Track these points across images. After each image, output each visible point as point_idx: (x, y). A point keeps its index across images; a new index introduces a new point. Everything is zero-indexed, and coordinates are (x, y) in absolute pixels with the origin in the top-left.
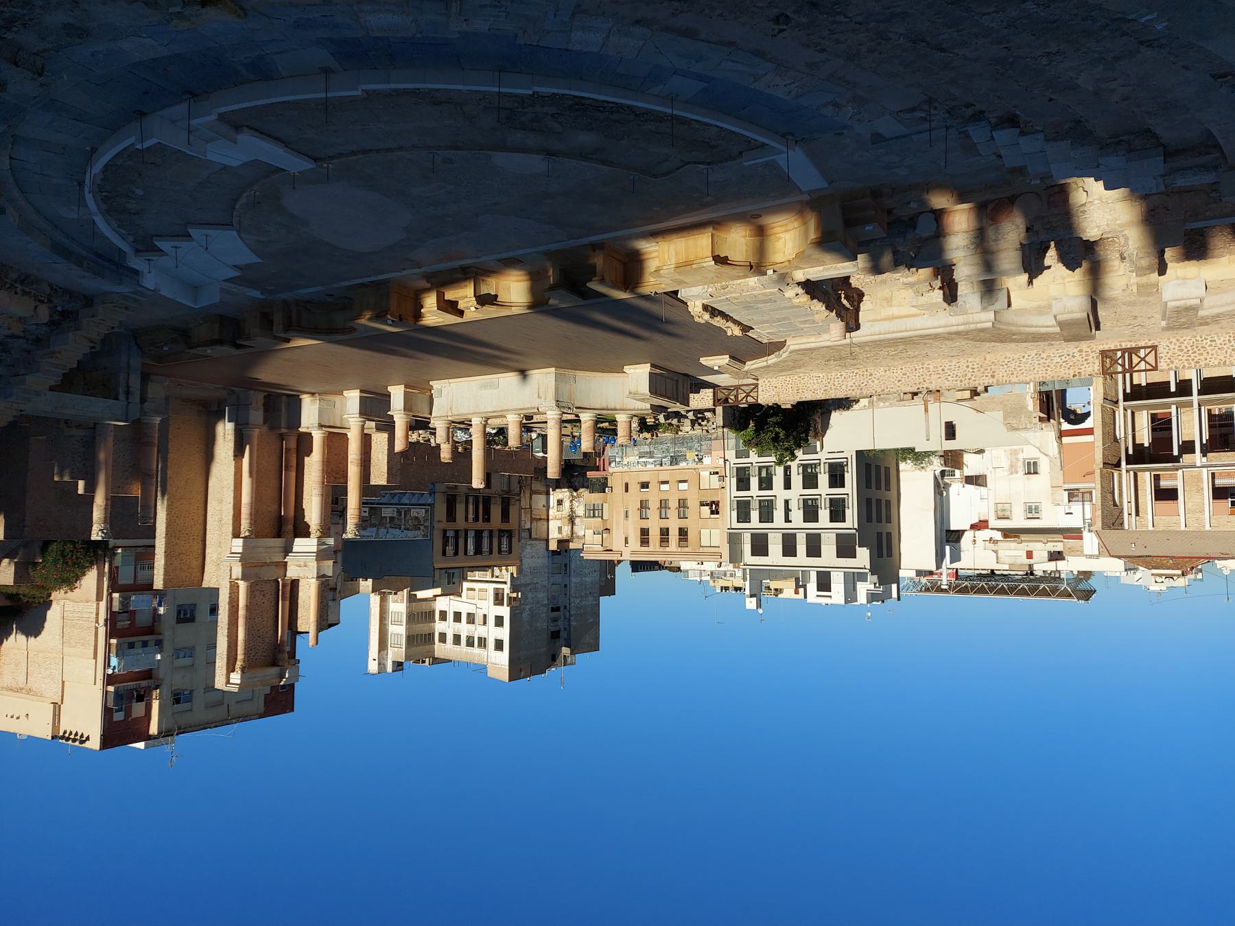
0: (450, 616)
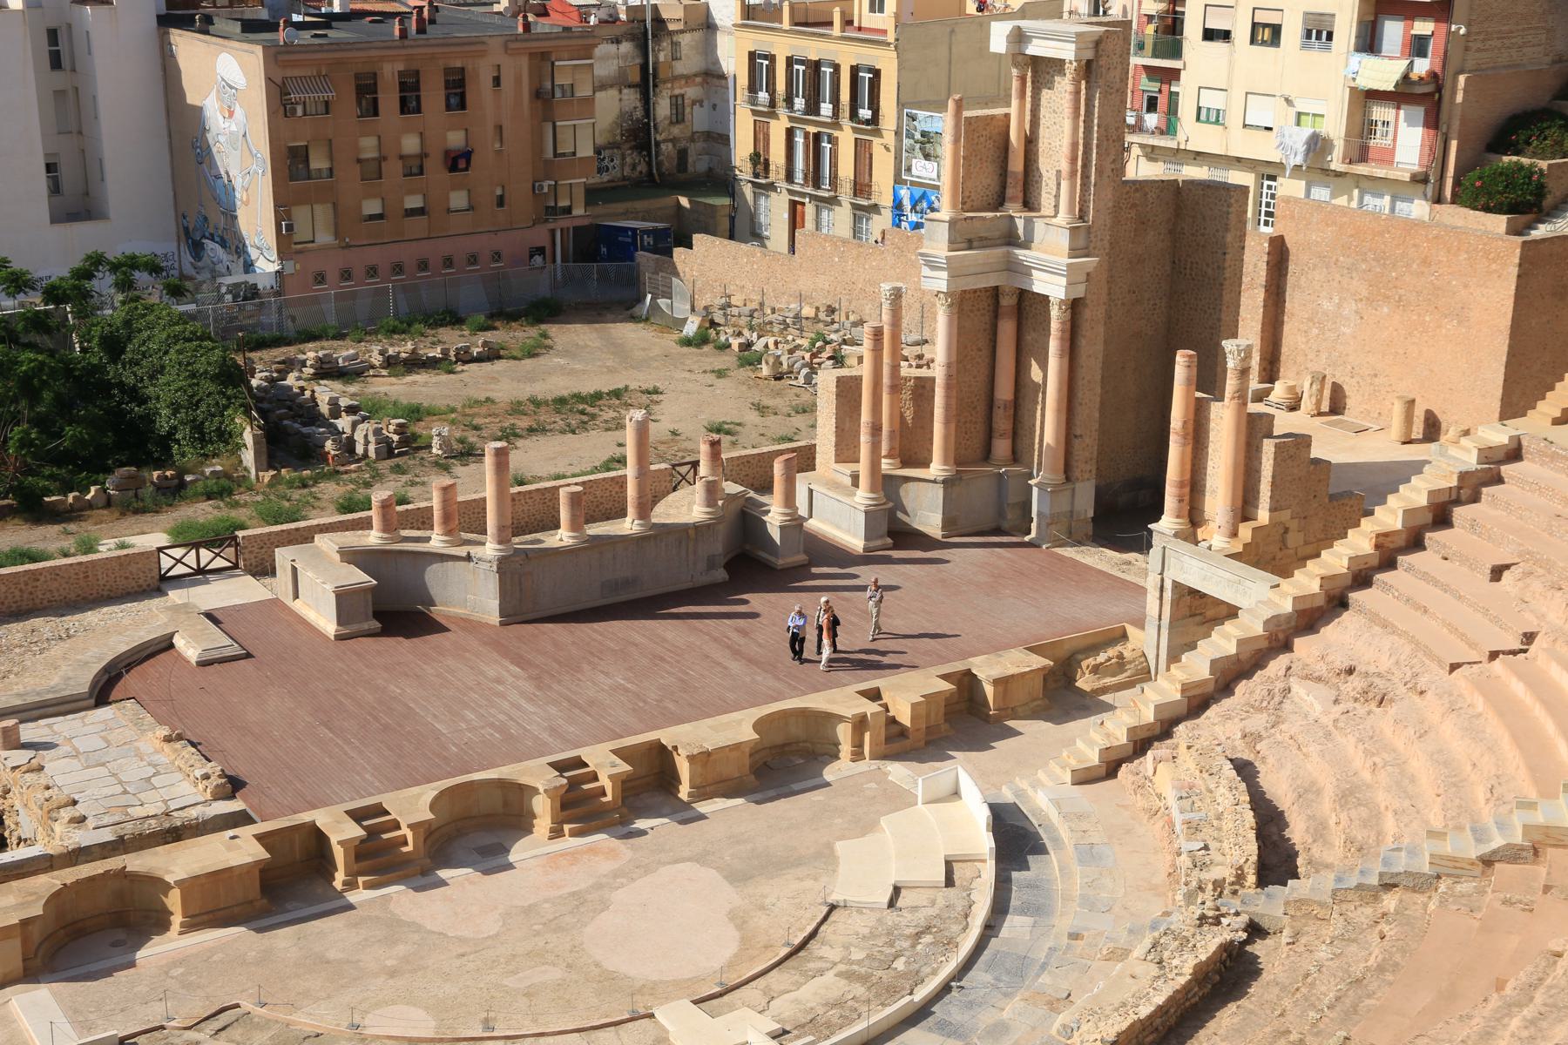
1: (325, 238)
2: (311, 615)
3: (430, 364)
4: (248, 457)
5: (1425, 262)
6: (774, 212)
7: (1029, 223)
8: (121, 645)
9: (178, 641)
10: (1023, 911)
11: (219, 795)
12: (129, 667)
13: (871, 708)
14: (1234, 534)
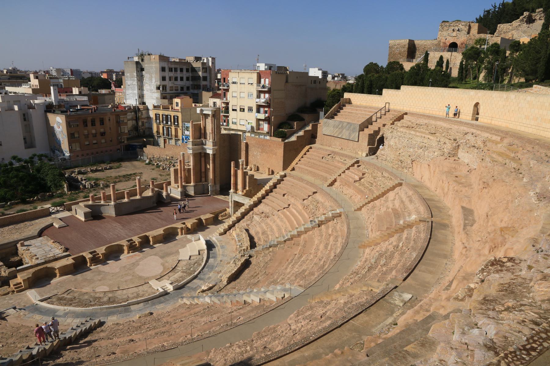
0: (185, 79)
1: (78, 149)
2: (80, 217)
3: (99, 171)
4: (66, 189)
5: (270, 146)
6: (161, 141)
7: (205, 141)
8: (43, 226)
9: (54, 224)
10: (212, 258)
11: (64, 251)
12: (45, 230)
13: (184, 226)
14: (243, 192)
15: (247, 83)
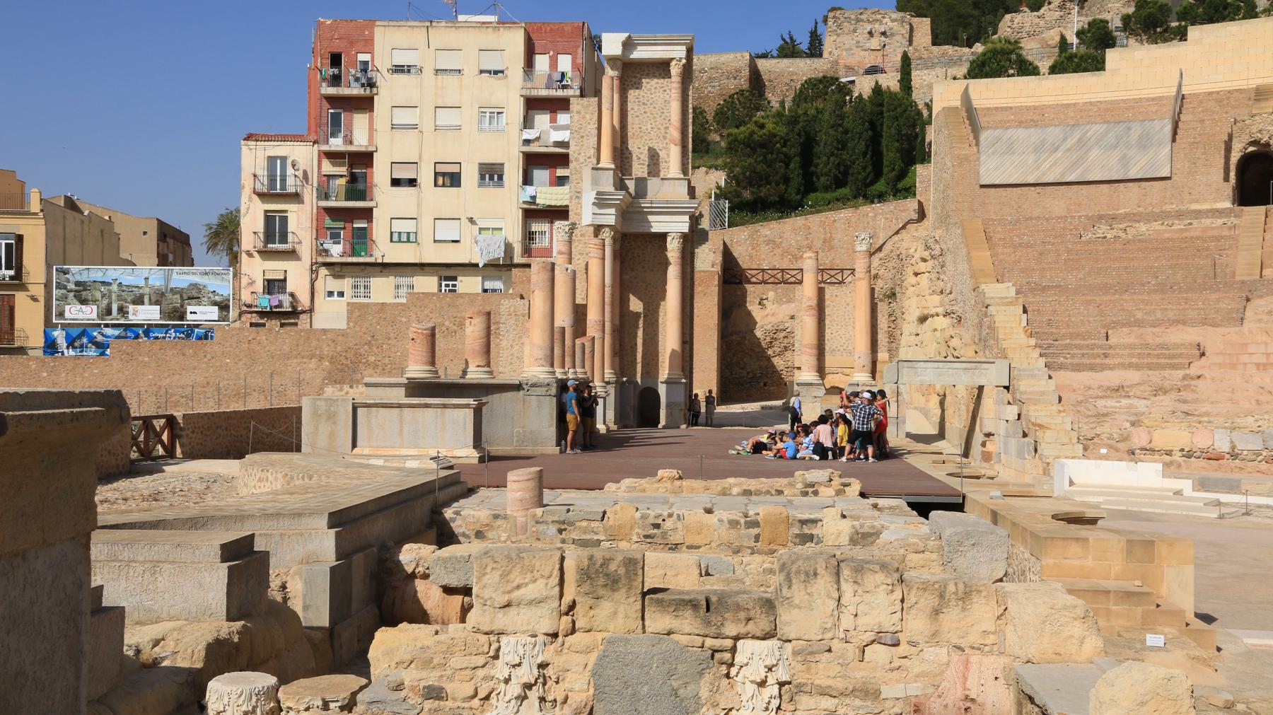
15: (470, 71)
